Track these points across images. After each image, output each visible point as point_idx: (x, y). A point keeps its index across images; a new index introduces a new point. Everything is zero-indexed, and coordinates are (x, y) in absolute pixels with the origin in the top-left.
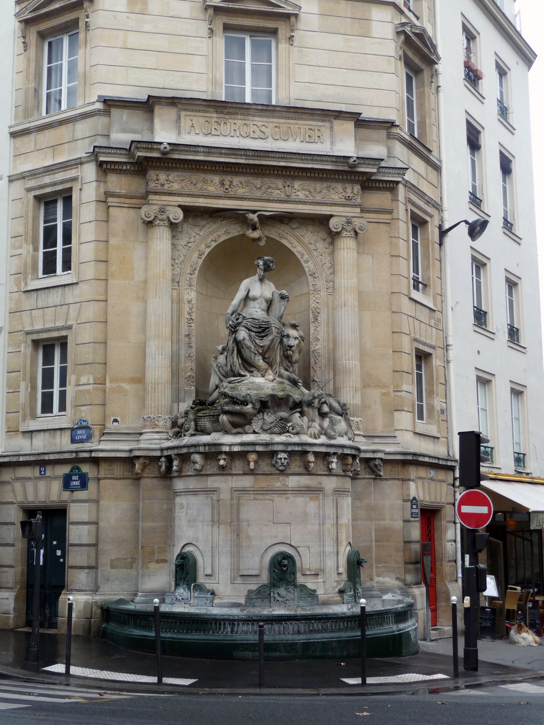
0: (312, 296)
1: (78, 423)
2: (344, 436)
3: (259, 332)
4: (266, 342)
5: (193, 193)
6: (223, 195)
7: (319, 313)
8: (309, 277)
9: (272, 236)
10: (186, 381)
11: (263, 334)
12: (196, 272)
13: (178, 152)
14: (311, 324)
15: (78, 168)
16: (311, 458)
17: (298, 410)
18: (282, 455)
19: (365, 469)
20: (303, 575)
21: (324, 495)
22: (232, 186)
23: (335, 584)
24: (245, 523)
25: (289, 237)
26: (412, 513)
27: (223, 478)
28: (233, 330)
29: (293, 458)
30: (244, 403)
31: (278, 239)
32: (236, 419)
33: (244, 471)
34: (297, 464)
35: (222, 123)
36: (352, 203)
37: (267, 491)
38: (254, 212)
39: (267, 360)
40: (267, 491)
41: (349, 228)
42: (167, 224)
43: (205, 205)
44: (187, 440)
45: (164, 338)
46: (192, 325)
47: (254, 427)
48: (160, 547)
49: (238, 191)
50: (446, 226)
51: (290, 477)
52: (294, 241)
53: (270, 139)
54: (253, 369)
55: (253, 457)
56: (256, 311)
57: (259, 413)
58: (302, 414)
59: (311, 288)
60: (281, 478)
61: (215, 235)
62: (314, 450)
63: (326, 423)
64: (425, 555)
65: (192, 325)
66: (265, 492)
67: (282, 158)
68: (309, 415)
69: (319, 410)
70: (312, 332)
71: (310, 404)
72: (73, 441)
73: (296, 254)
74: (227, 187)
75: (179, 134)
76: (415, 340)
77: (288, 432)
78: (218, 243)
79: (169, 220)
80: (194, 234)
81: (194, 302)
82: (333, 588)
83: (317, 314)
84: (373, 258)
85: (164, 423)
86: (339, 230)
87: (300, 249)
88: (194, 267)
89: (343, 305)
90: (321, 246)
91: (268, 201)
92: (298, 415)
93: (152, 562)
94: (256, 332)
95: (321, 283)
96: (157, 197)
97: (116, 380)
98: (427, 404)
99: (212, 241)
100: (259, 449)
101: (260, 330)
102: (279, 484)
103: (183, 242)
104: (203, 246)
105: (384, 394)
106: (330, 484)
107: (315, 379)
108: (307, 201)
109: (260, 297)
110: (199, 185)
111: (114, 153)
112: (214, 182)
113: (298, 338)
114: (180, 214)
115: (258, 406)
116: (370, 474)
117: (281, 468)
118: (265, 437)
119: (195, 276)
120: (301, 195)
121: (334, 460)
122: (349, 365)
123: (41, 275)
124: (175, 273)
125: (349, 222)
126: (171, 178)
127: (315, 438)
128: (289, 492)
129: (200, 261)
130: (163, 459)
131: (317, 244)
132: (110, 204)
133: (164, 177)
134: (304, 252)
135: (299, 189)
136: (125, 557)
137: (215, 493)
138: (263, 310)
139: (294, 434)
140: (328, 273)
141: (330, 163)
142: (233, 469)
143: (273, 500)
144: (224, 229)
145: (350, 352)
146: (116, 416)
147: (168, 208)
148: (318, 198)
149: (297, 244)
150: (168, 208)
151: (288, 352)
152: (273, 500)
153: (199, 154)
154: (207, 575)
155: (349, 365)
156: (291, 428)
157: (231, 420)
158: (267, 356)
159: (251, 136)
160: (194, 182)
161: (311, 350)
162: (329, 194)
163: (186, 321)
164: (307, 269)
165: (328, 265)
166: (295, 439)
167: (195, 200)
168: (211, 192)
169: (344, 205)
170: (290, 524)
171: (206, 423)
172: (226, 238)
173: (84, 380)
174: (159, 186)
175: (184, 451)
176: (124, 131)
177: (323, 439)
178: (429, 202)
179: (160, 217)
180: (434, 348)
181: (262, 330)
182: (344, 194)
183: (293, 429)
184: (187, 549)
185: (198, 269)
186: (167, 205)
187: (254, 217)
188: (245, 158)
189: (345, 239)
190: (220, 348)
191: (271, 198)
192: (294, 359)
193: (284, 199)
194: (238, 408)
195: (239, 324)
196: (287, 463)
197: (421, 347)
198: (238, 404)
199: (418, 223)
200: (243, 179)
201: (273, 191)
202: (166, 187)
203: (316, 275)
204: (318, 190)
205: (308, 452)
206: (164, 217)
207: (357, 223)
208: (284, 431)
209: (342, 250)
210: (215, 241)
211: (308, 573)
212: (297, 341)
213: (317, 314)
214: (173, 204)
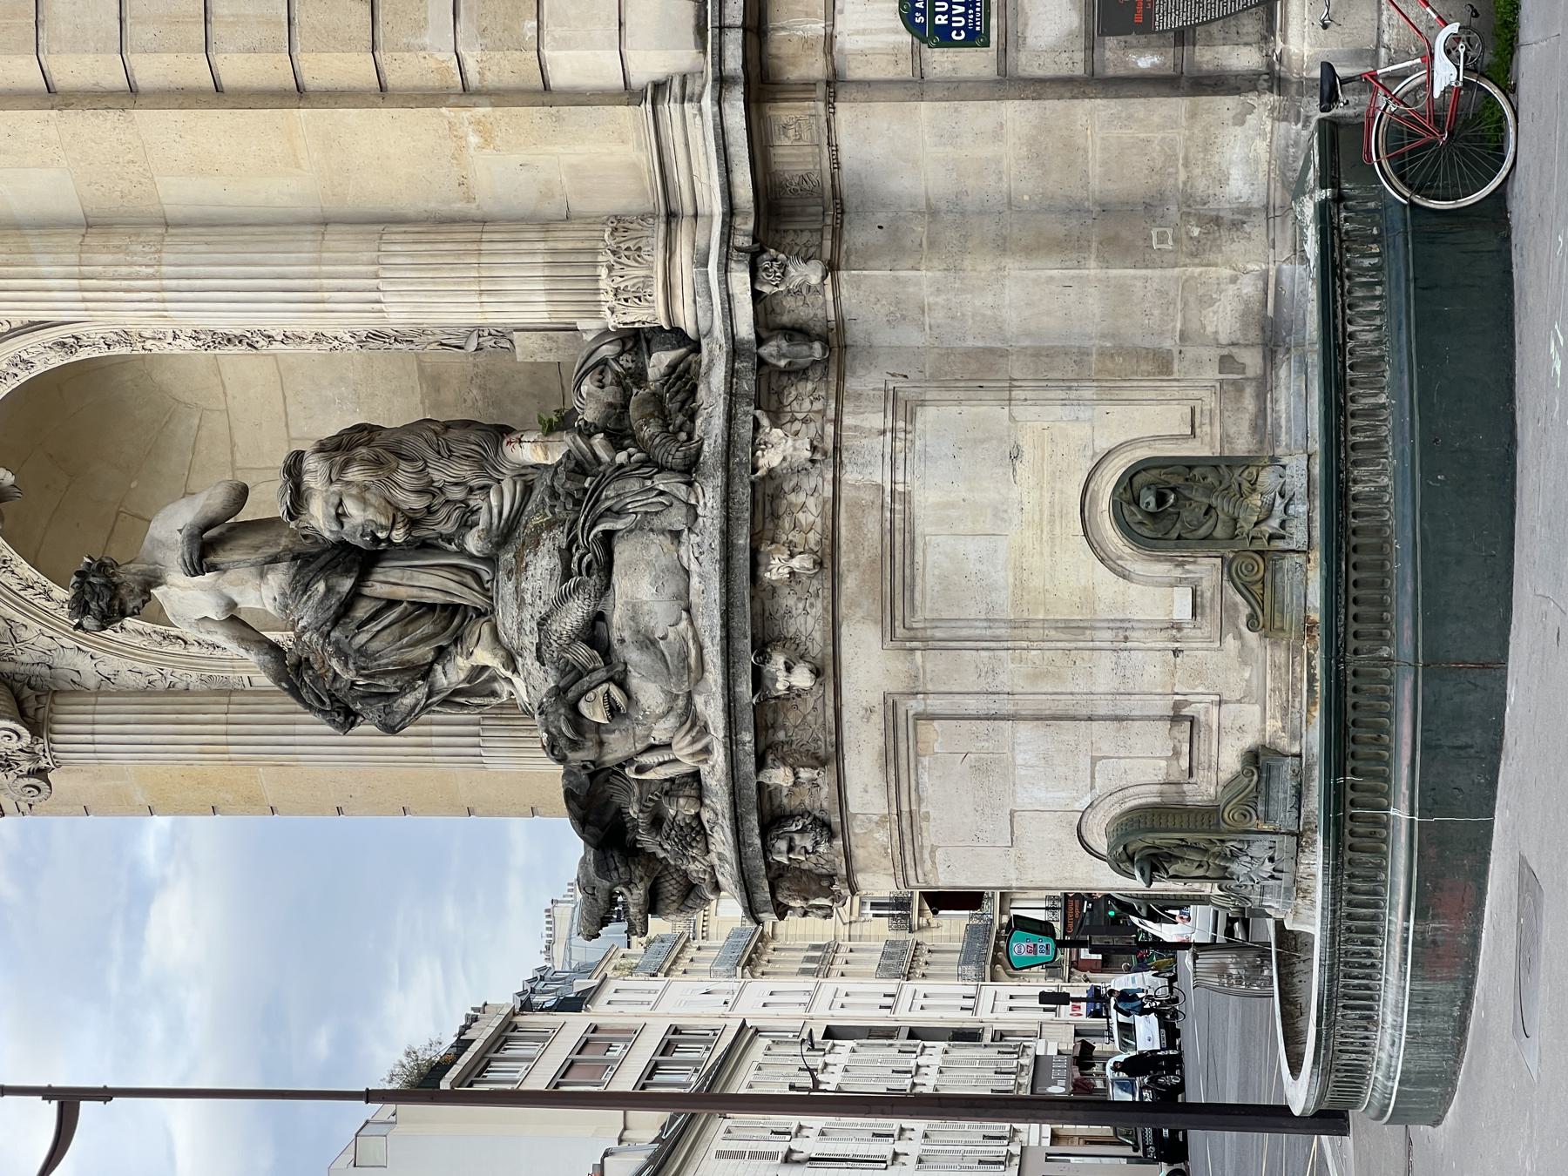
16: (779, 777)
20: (1191, 774)
23: (1231, 642)
26: (975, 38)
29: (785, 801)
32: (671, 887)
40: (902, 854)
51: (854, 806)
60: (856, 829)
63: (650, 694)
77: (698, 816)
78: (51, 584)
82: (1244, 657)
88: (159, 639)
99: (49, 599)
102: (881, 836)
103: (84, 663)
107: (472, 346)
113: (341, 503)
127: (707, 750)
128: (905, 808)
139: (700, 799)
170: (1012, 813)
177: (711, 709)
184: (1102, 845)
185: (158, 628)
196: (802, 831)
208: (697, 832)
211: (1185, 764)
212: (351, 507)
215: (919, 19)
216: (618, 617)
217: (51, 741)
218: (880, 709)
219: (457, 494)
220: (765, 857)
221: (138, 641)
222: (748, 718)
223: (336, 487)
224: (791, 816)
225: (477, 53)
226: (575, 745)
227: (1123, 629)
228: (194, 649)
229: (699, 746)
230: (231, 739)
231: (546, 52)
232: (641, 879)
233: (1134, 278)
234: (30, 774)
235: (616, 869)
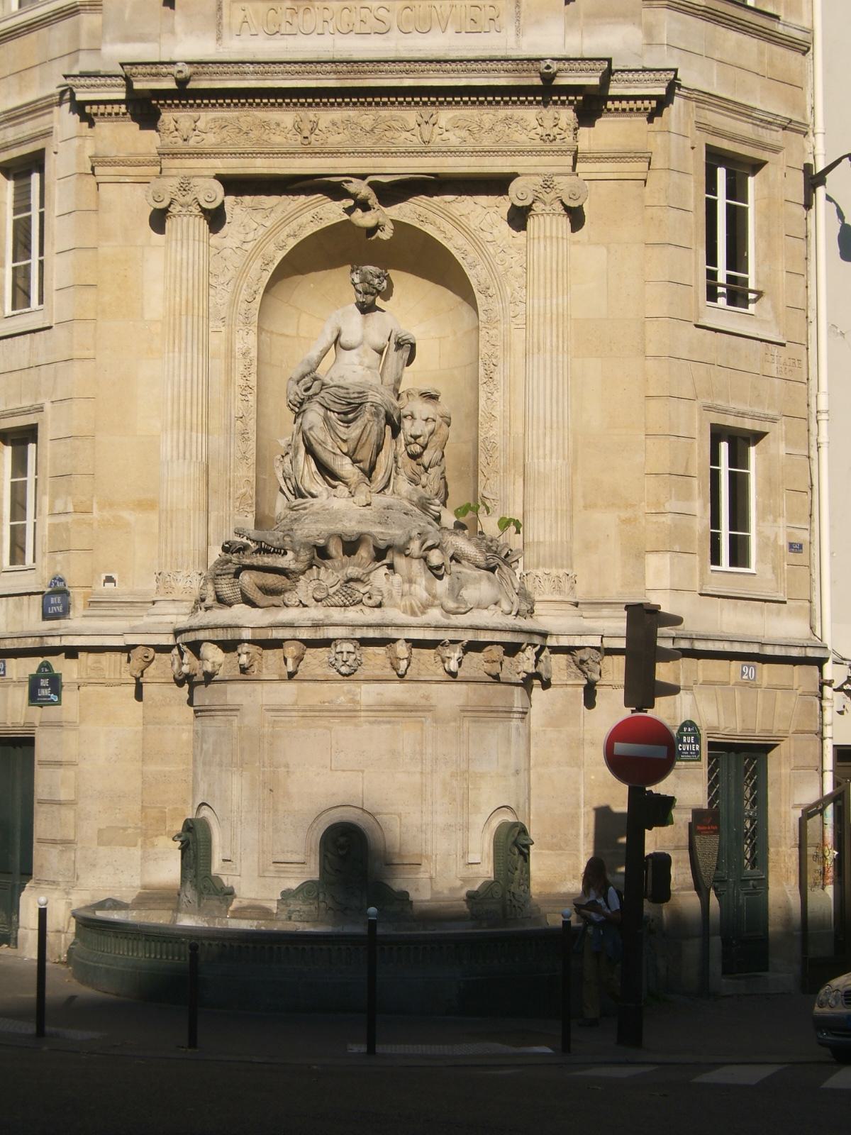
1: (51, 584)
2: (492, 607)
3: (346, 414)
4: (354, 432)
6: (300, 150)
10: (238, 504)
11: (351, 416)
13: (207, 77)
14: (481, 388)
15: (51, 112)
16: (402, 649)
19: (568, 666)
21: (436, 721)
24: (283, 769)
25: (439, 220)
27: (248, 687)
28: (297, 410)
30: (282, 551)
31: (418, 226)
32: (271, 580)
33: (280, 675)
34: (378, 662)
35: (302, 10)
36: (554, 148)
37: (320, 711)
38: (363, 177)
40: (320, 711)
41: (547, 198)
42: (196, 212)
43: (265, 171)
44: (204, 618)
45: (188, 427)
46: (250, 398)
47: (300, 594)
48: (176, 809)
49: (329, 140)
50: (820, 167)
51: (365, 687)
53: (395, 33)
54: (336, 483)
56: (352, 371)
57: (310, 567)
60: (347, 686)
61: (294, 225)
62: (407, 637)
63: (442, 586)
64: (699, 832)
66: (317, 714)
67: (407, 72)
69: (425, 559)
71: (403, 550)
72: (46, 616)
73: (453, 251)
74: (306, 133)
75: (219, 39)
76: (708, 408)
78: (300, 239)
80: (255, 226)
81: (254, 354)
84: (609, 251)
85: (190, 582)
86: (527, 203)
87: (460, 243)
88: (255, 288)
89: (536, 350)
91: (386, 154)
92: (384, 570)
93: (162, 835)
94: (339, 413)
96: (177, 162)
97: (111, 505)
98: (759, 533)
99: (288, 236)
101: (345, 409)
104: (271, 247)
105: (626, 521)
106: (451, 697)
108: (463, 149)
109: (361, 343)
112: (282, 125)
113: (434, 421)
115: (305, 556)
116: (577, 677)
117: (344, 670)
118: (316, 613)
119: (256, 305)
120: (453, 138)
121: (452, 654)
122: (545, 468)
123: (8, 310)
124: (219, 301)
125: (547, 186)
127: (413, 613)
128: (363, 714)
130: (175, 651)
131: (495, 231)
132: (100, 179)
133: (187, 124)
134: (468, 248)
135: (448, 128)
136: (124, 825)
137: (238, 713)
138: (369, 368)
140: (517, 285)
141: (503, 74)
142: (264, 670)
143: (329, 729)
144: (312, 211)
145: (548, 440)
146: (111, 572)
147: (194, 181)
148: (487, 142)
150: (194, 181)
151: (412, 446)
152: (329, 729)
154: (224, 860)
155: (545, 468)
156: (367, 595)
157: (260, 582)
158: (359, 458)
159: (357, 29)
160: (245, 129)
161: (481, 439)
162: (508, 131)
163: (238, 390)
164: (473, 282)
166: (374, 616)
167: (246, 162)
169: (539, 153)
171: (226, 589)
172: (316, 229)
173: (59, 507)
174: (180, 141)
175: (190, 637)
176: (127, 39)
177: (435, 615)
178: (767, 122)
179: (182, 200)
180: (774, 420)
181: (351, 408)
182: (540, 130)
183: (370, 598)
186: (193, 177)
187: (360, 188)
188: (335, 76)
189: (541, 218)
190: (283, 443)
191: (393, 150)
192: (426, 459)
193: (418, 149)
194: (268, 560)
195: (310, 398)
197: (730, 421)
198: (267, 551)
199: (731, 167)
201: (397, 135)
202: (192, 142)
203: (490, 292)
204: (487, 126)
205: (395, 641)
206: (189, 199)
207: (564, 185)
209: (536, 241)
210: (295, 236)
212: (431, 426)
214: (206, 173)
215: (685, 729)
216: (466, 570)
217: (196, 216)
218: (428, 703)
219: (424, 479)
223: (439, 420)
225: (669, 522)
227: (466, 827)
229: (416, 609)
230: (196, 318)
231: (668, 555)
233: (578, 829)
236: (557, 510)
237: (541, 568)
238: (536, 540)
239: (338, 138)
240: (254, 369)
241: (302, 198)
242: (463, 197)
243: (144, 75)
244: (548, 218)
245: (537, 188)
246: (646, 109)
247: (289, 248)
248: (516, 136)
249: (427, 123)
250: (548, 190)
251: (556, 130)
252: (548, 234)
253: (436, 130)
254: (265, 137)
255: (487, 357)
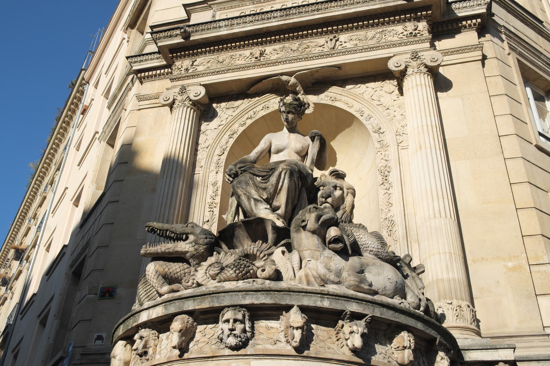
0: (379, 153)
5: (218, 70)
7: (389, 172)
8: (373, 134)
9: (322, 102)
12: (226, 153)
17: (283, 242)
18: (229, 314)
22: (264, 55)
25: (343, 98)
31: (330, 103)
39: (279, 212)
46: (215, 210)
52: (350, 101)
55: (176, 325)
58: (289, 248)
59: (378, 145)
61: (251, 113)
65: (215, 210)
67: (318, 10)
68: (300, 245)
70: (381, 196)
73: (354, 113)
78: (254, 120)
79: (190, 100)
81: (220, 184)
83: (386, 173)
84: (463, 100)
88: (224, 147)
90: (387, 100)
91: (307, 59)
94: (262, 176)
95: (389, 138)
99: (248, 118)
100: (190, 305)
110: (227, 61)
111: (146, 60)
114: (203, 91)
125: (415, 56)
126: (195, 64)
129: (232, 141)
131: (382, 100)
134: (363, 109)
135: (346, 41)
142: (157, 357)
144: (263, 105)
148: (372, 43)
149: (355, 103)
153: (222, 29)
157: (161, 270)
163: (207, 206)
164: (369, 127)
165: (399, 117)
168: (240, 65)
172: (264, 114)
174: (183, 72)
185: (228, 149)
189: (413, 77)
196: (244, 331)
200: (277, 46)
203: (381, 131)
206: (185, 97)
210: (251, 118)
213: (386, 173)
220: (228, 307)
221: (224, 141)
222: (338, 305)
224: (252, 328)
226: (318, 218)
228: (216, 158)
229: (312, 279)
232: (196, 250)
234: (174, 100)
235: (206, 238)
236: (450, 253)
237: (443, 300)
238: (435, 279)
239: (278, 56)
240: (219, 192)
241: (257, 98)
242: (359, 85)
243: (165, 37)
244: (418, 75)
245: (407, 60)
246: (475, 24)
247: (247, 125)
248: (390, 39)
249: (331, 40)
250: (415, 59)
251: (417, 32)
252: (419, 83)
253: (338, 43)
254: (232, 62)
255: (382, 168)
